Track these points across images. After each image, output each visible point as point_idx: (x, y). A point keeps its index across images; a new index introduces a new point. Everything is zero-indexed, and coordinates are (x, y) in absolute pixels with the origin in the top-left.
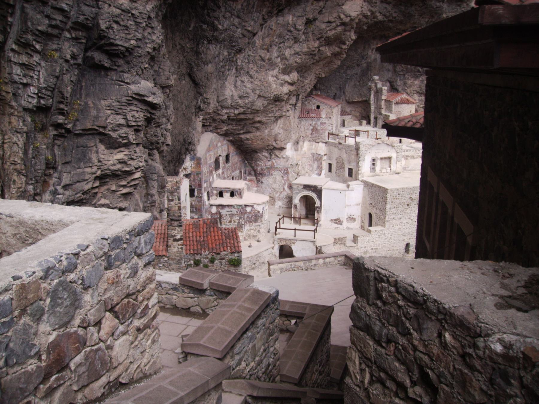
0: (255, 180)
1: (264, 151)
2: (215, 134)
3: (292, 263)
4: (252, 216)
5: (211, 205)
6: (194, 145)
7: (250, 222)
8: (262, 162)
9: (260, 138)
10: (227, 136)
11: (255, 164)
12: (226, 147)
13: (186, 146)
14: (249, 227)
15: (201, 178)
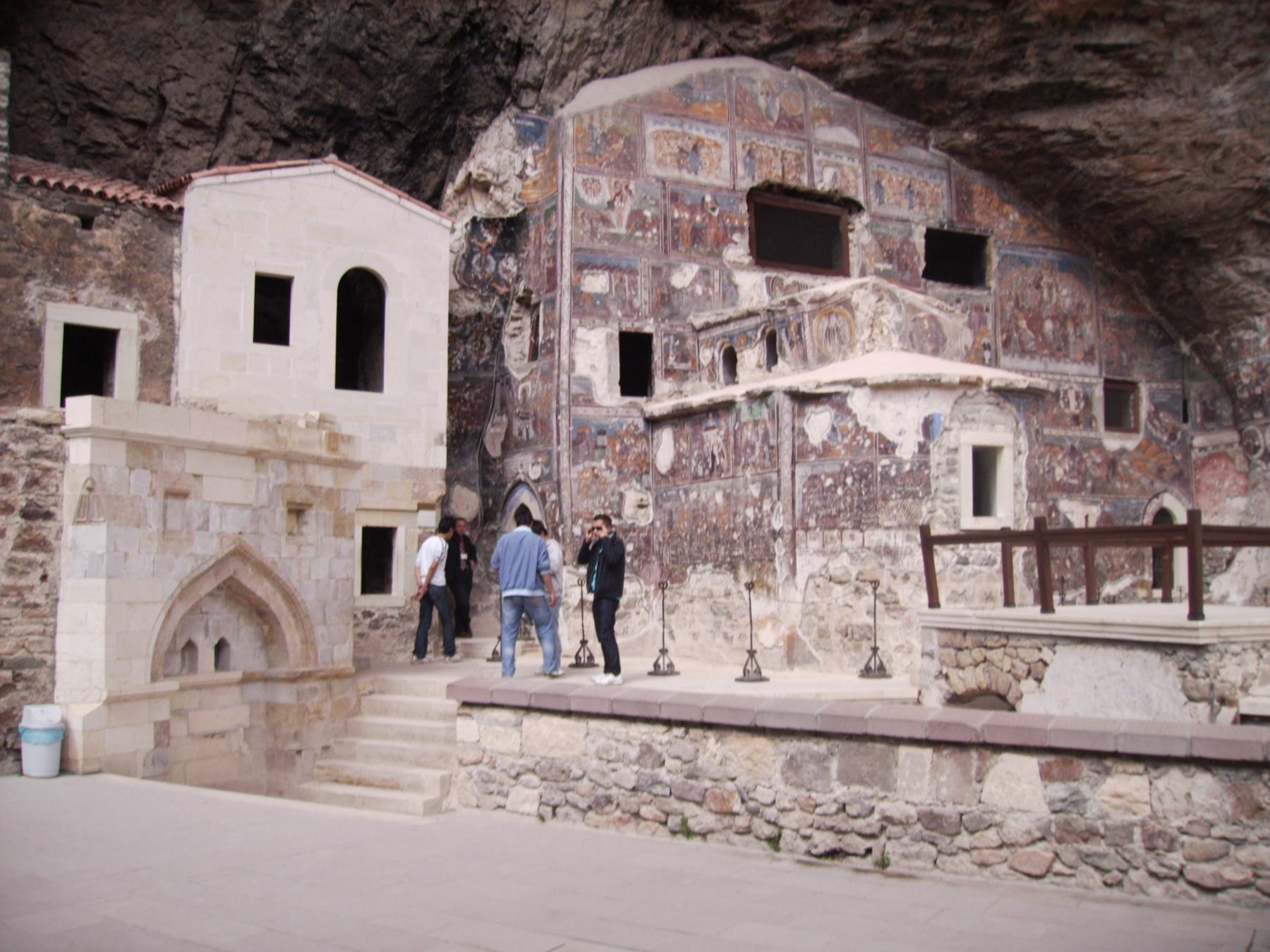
0: (1236, 452)
1: (1248, 236)
2: (802, 75)
3: (658, 735)
4: (839, 479)
5: (653, 422)
6: (538, 53)
7: (829, 522)
8: (1261, 323)
9: (1183, 137)
10: (936, 121)
11: (1227, 347)
12: (936, 187)
13: (504, 70)
14: (819, 561)
15: (555, 233)
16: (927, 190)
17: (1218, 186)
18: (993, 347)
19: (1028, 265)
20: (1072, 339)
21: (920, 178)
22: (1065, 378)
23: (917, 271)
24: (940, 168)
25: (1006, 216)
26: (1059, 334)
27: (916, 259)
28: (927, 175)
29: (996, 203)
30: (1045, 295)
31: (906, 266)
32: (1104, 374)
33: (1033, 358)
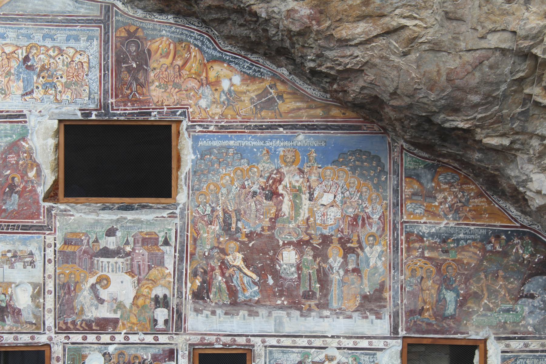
16: (60, 63)
17: (463, 45)
18: (173, 302)
19: (253, 161)
20: (336, 277)
21: (49, 43)
22: (318, 342)
23: (33, 191)
24: (88, 21)
25: (215, 84)
26: (310, 270)
27: (32, 174)
28: (61, 35)
29: (194, 65)
30: (286, 207)
31: (12, 187)
32: (402, 333)
33: (253, 314)
